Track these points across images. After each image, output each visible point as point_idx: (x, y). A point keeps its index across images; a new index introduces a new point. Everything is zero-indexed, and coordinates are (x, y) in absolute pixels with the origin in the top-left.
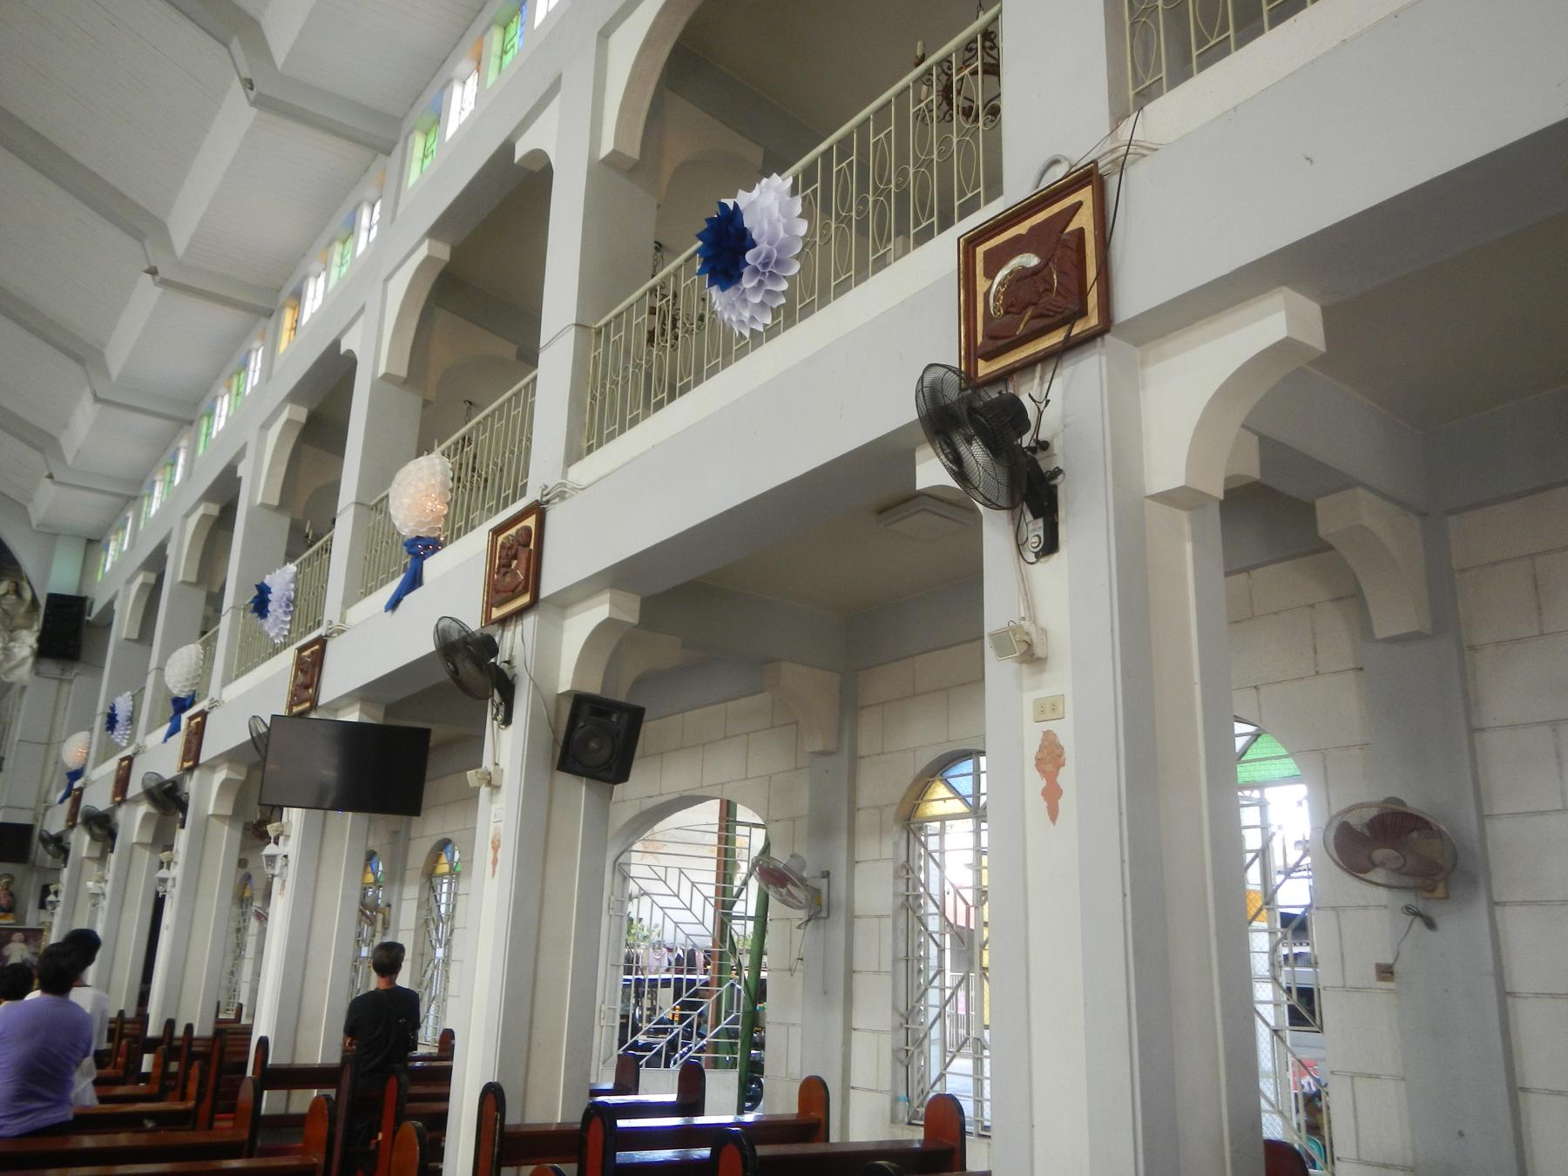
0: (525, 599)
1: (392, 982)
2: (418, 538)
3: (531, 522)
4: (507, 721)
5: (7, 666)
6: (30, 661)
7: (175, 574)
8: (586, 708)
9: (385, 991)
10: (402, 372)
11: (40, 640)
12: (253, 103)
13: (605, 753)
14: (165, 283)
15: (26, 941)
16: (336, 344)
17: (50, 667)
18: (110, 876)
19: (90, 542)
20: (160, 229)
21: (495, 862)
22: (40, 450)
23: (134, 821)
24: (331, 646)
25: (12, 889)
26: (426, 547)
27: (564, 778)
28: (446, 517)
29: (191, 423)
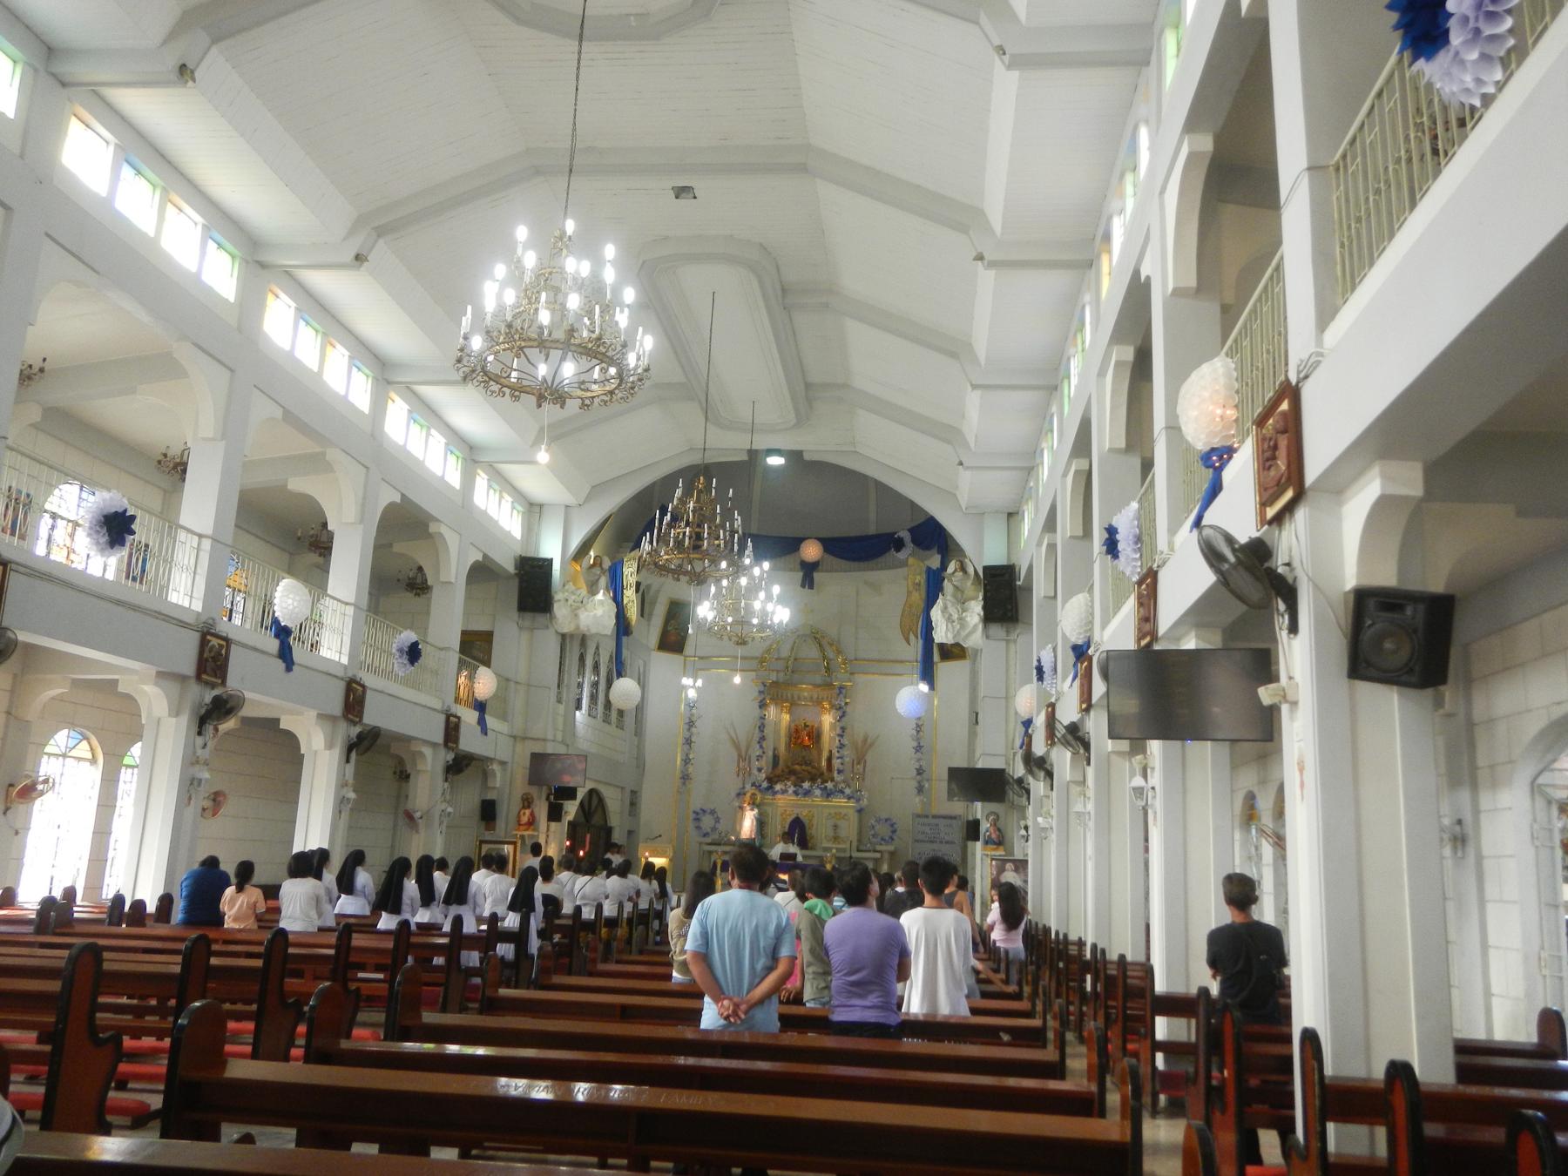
0: (1289, 494)
1: (1248, 915)
2: (1213, 450)
3: (1285, 406)
4: (1293, 629)
5: (963, 634)
6: (980, 626)
7: (1064, 528)
8: (1371, 604)
9: (1242, 925)
10: (1192, 282)
11: (985, 608)
12: (1009, 67)
13: (1405, 654)
14: (992, 265)
15: (1016, 870)
16: (1136, 273)
17: (997, 630)
18: (1054, 812)
19: (1010, 515)
20: (979, 213)
21: (1302, 785)
22: (949, 442)
23: (1062, 759)
24: (1161, 576)
25: (1000, 824)
26: (1221, 458)
27: (1366, 689)
28: (1236, 421)
29: (1056, 388)
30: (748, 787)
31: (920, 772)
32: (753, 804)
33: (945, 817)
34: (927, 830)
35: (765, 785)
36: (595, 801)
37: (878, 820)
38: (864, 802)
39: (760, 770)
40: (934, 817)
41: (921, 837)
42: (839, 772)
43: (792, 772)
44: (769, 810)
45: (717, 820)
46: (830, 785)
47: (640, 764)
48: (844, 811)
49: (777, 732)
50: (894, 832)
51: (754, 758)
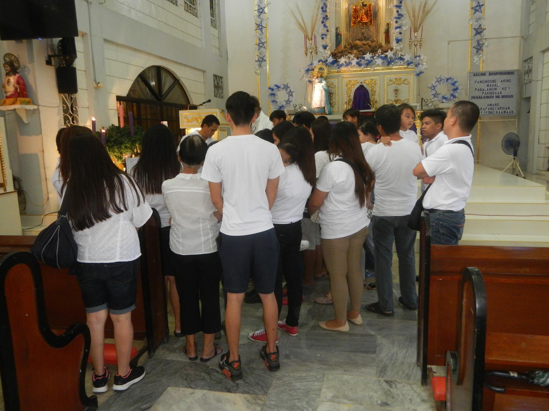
30: (315, 63)
31: (479, 31)
32: (321, 77)
33: (501, 73)
34: (484, 86)
35: (331, 59)
36: (167, 83)
37: (439, 81)
38: (422, 68)
39: (325, 47)
40: (491, 74)
41: (479, 94)
42: (398, 41)
43: (353, 47)
44: (335, 81)
45: (291, 94)
46: (390, 54)
47: (223, 54)
48: (403, 77)
49: (337, 12)
50: (456, 90)
51: (319, 38)
